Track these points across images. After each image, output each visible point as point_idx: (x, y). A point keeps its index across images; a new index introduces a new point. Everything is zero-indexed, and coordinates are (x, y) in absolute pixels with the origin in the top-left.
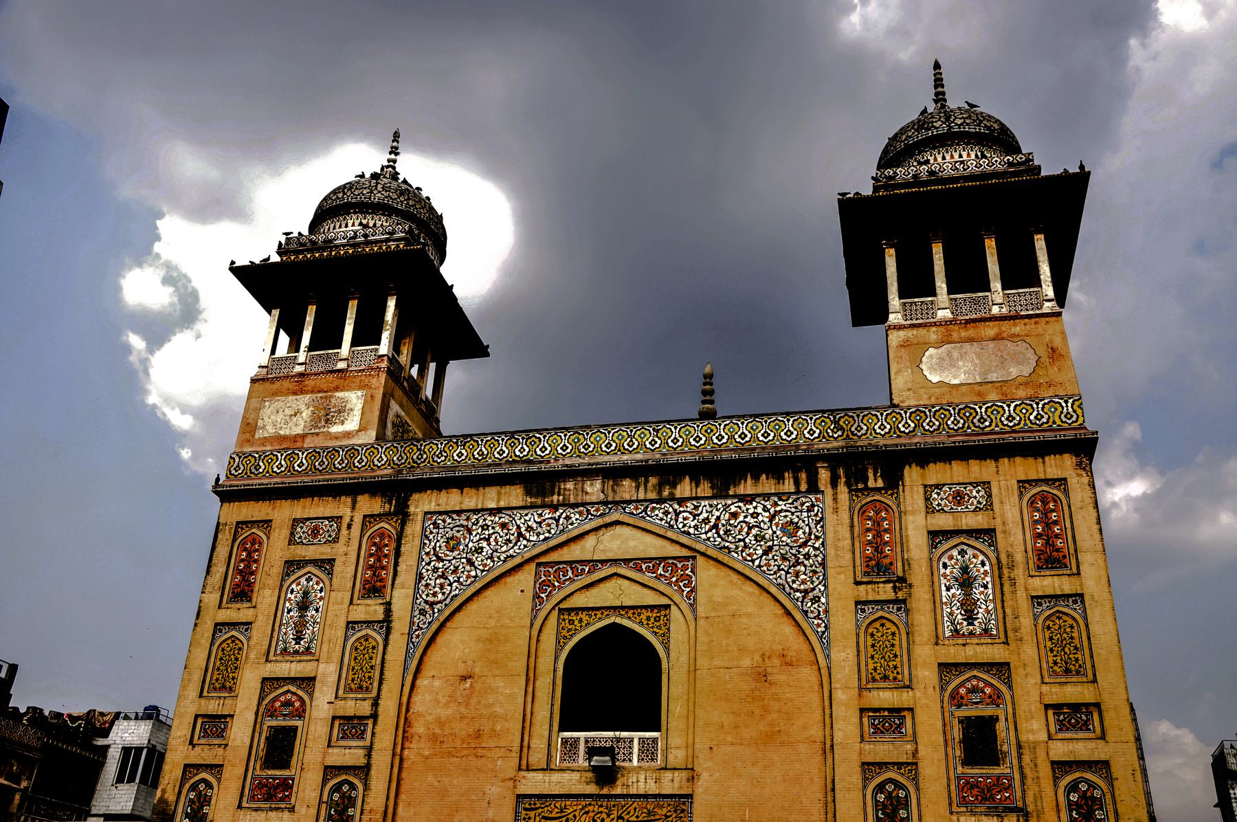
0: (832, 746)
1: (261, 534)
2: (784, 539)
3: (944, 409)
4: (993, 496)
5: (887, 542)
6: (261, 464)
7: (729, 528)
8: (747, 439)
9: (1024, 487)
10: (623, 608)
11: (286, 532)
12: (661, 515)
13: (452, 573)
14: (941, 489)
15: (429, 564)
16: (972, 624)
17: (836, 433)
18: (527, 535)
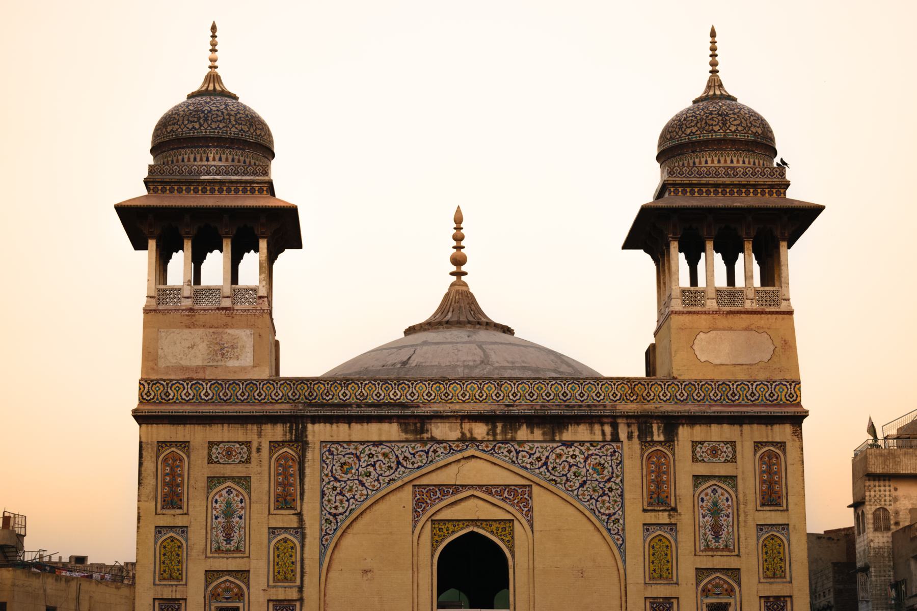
1: (181, 453)
2: (595, 475)
3: (708, 384)
4: (737, 452)
5: (665, 481)
6: (169, 391)
7: (555, 465)
8: (568, 397)
9: (757, 446)
10: (478, 520)
11: (206, 452)
12: (505, 451)
13: (348, 492)
14: (702, 444)
15: (329, 483)
16: (718, 542)
17: (632, 397)
18: (404, 463)
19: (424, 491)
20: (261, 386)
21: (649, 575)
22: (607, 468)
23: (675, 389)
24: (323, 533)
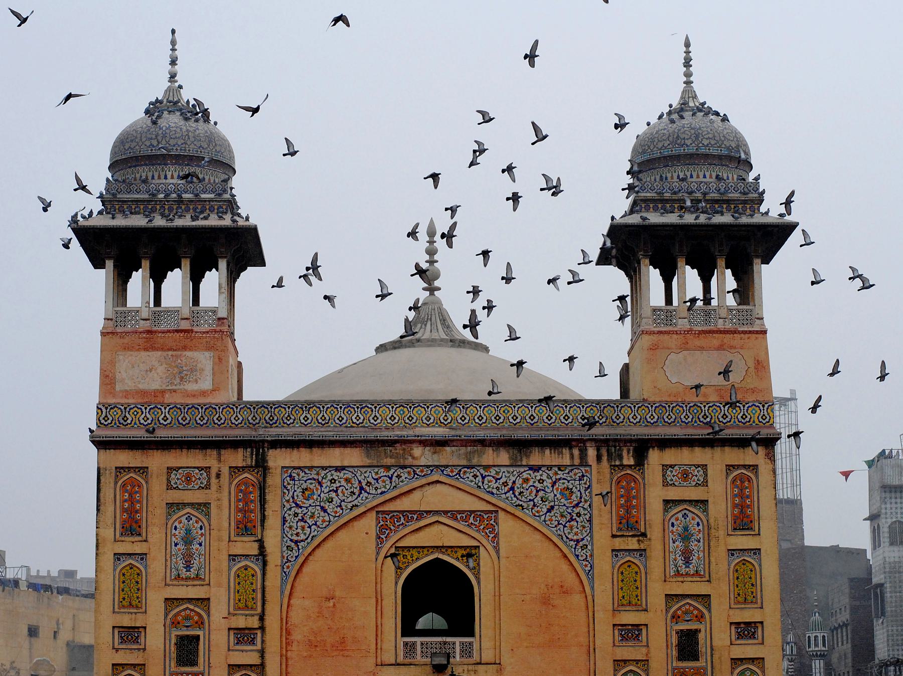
0: (595, 649)
1: (139, 479)
2: (563, 500)
3: (679, 406)
4: (708, 476)
5: (634, 506)
6: (127, 415)
7: (522, 490)
8: (535, 420)
9: (729, 469)
10: (443, 547)
11: (164, 478)
12: (471, 478)
14: (673, 468)
15: (290, 509)
16: (687, 567)
17: (601, 420)
18: (367, 488)
19: (388, 517)
20: (221, 410)
21: (618, 601)
22: (575, 493)
23: (645, 412)
24: (285, 560)
